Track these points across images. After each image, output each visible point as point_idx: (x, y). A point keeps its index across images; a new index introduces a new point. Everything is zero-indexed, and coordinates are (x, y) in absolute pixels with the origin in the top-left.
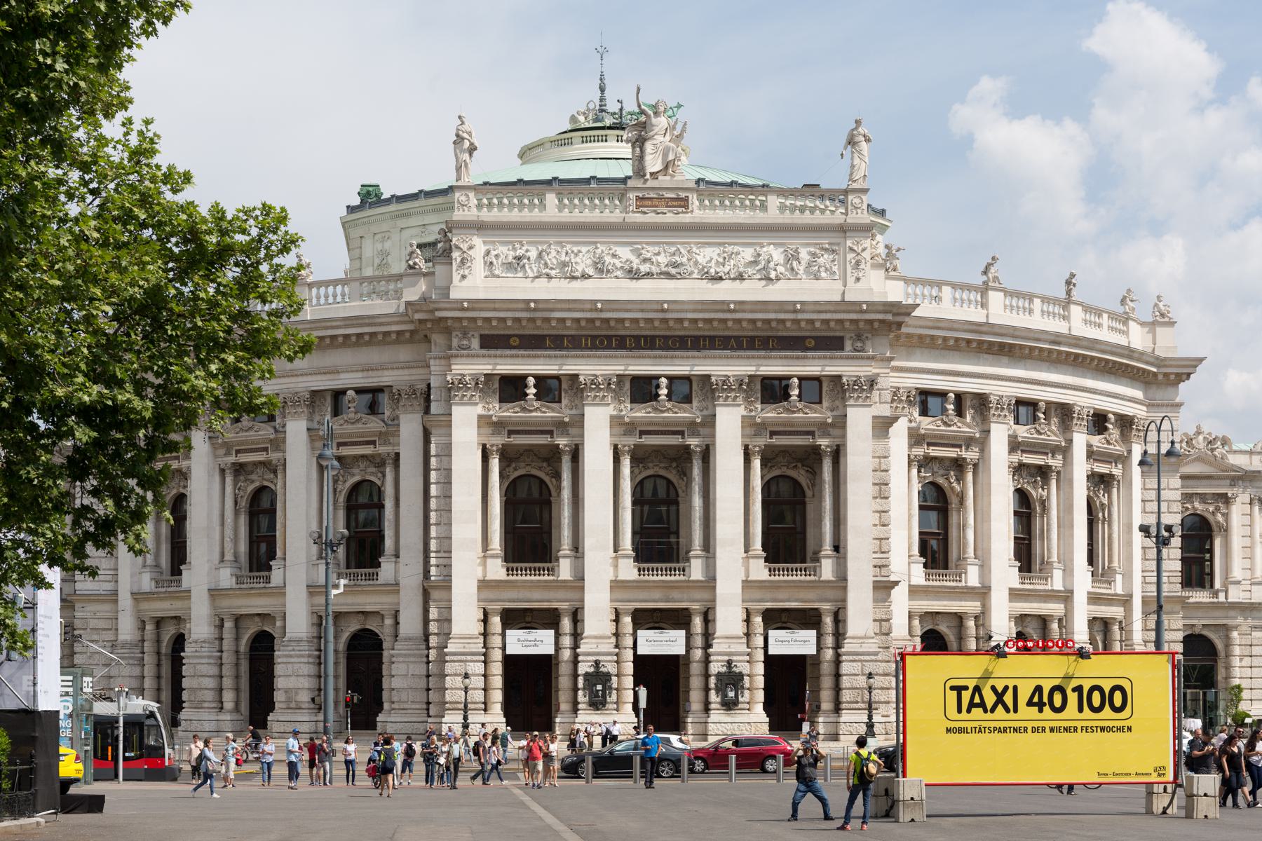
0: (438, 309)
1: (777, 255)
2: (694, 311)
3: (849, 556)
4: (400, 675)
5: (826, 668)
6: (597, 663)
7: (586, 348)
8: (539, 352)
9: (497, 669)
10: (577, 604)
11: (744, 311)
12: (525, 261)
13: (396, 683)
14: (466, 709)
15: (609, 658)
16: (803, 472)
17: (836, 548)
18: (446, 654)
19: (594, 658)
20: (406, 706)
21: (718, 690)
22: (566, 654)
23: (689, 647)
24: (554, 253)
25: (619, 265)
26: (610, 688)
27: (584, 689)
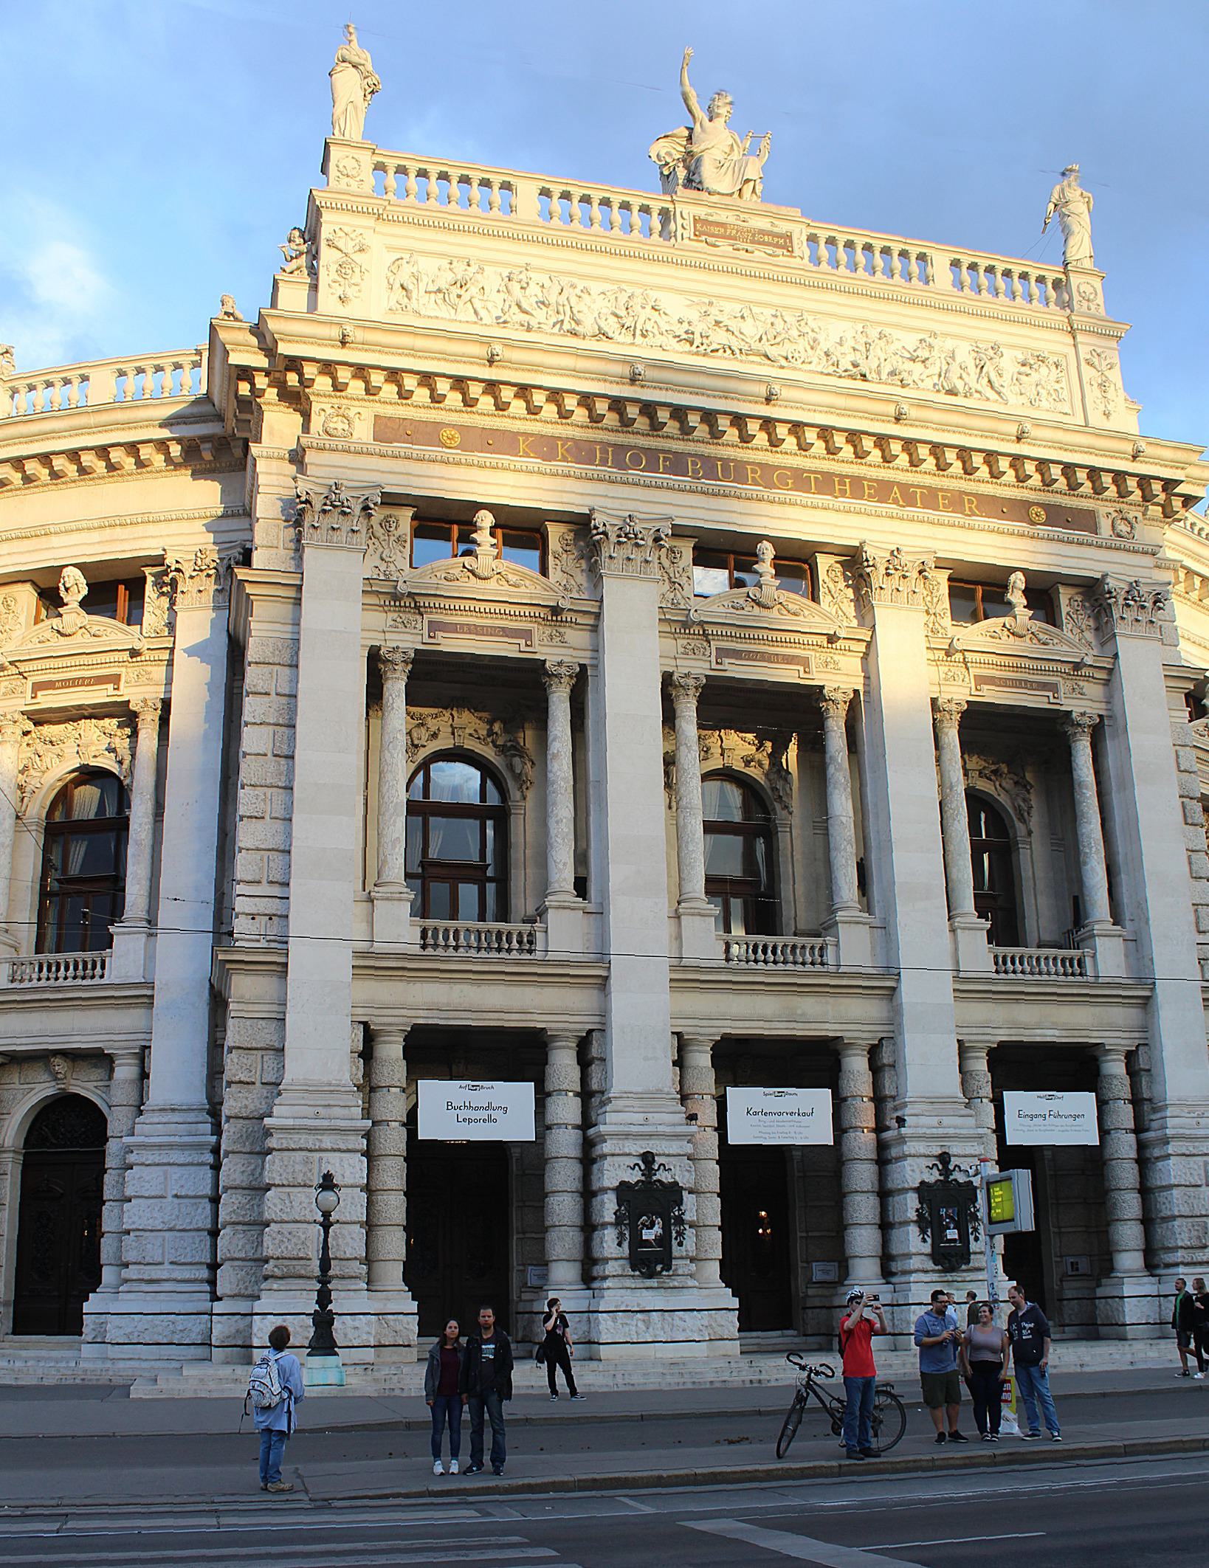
0: (292, 338)
1: (964, 355)
2: (831, 409)
3: (1155, 930)
4: (147, 1197)
5: (1126, 1174)
6: (648, 1158)
7: (604, 462)
8: (505, 459)
9: (394, 1174)
10: (587, 1023)
11: (924, 423)
12: (473, 290)
13: (135, 1215)
14: (324, 1279)
15: (674, 1147)
16: (1008, 784)
17: (1117, 918)
18: (268, 1133)
19: (639, 1147)
20: (155, 1273)
21: (922, 1223)
22: (565, 1143)
23: (840, 1128)
24: (533, 289)
25: (664, 327)
26: (680, 1220)
27: (618, 1223)
